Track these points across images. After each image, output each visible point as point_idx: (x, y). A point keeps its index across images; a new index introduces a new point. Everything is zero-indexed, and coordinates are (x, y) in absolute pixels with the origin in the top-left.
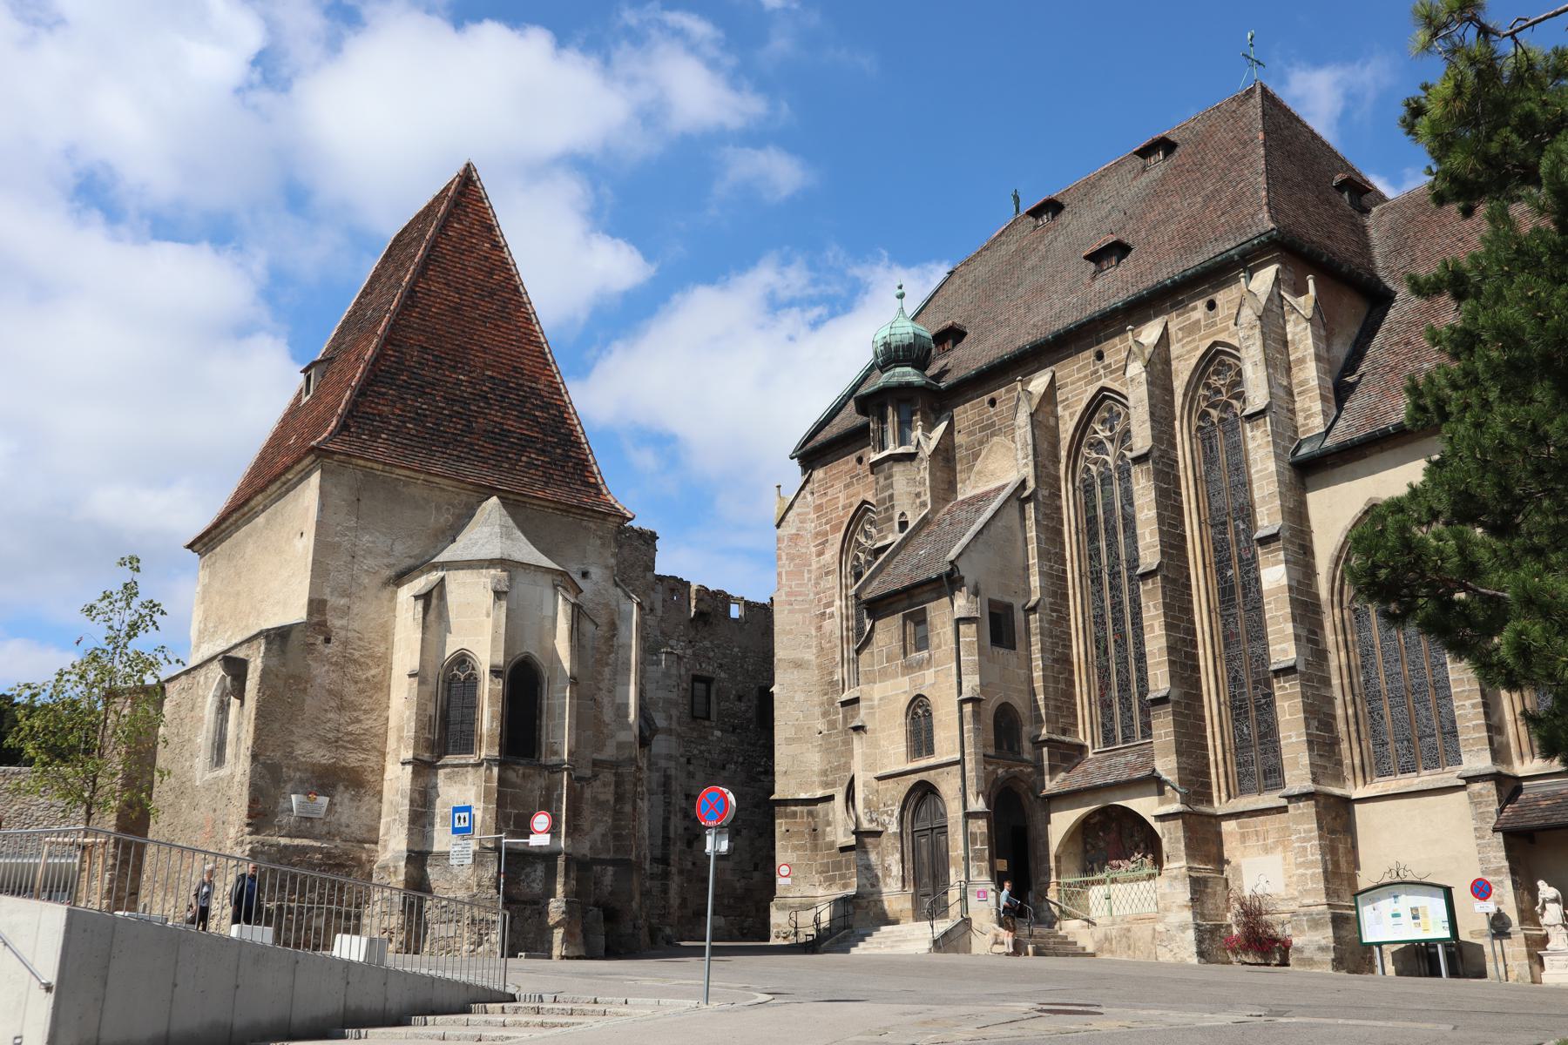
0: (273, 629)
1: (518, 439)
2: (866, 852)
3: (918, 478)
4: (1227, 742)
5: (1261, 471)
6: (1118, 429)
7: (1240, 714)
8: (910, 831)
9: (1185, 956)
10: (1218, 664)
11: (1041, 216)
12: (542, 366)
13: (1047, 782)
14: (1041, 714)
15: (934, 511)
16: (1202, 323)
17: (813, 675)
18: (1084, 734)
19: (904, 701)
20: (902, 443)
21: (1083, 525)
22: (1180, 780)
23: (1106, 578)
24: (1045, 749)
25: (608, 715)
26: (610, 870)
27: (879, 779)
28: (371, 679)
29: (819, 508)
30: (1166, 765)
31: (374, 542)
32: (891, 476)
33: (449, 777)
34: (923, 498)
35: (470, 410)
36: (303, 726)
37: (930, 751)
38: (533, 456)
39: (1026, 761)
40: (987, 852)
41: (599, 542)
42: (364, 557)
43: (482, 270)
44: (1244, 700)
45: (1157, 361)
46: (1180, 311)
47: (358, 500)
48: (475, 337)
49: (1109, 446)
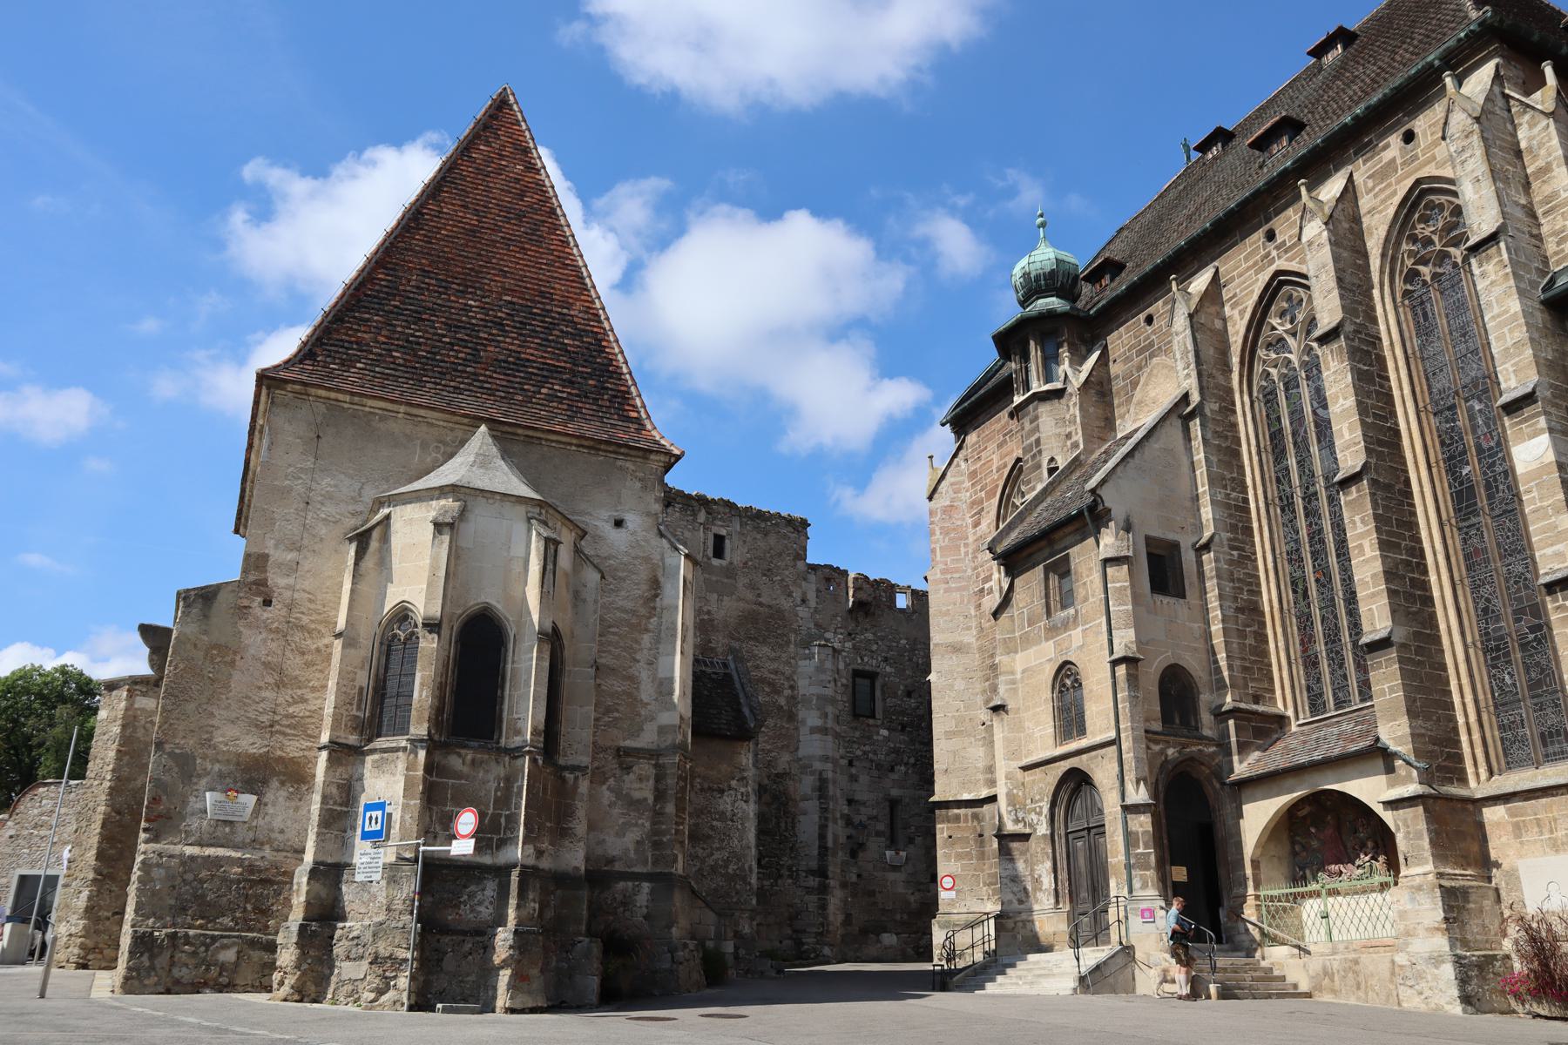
0: (194, 589)
1: (539, 369)
2: (1012, 860)
3: (1068, 417)
4: (1481, 697)
5: (1499, 316)
6: (1300, 317)
7: (1497, 658)
8: (1063, 833)
9: (1442, 1002)
10: (1460, 592)
11: (1210, 149)
12: (578, 291)
13: (1236, 764)
14: (1223, 678)
15: (1088, 451)
16: (1399, 161)
17: (974, 660)
18: (1282, 703)
19: (1049, 671)
20: (1048, 380)
21: (1266, 442)
22: (1416, 752)
23: (1299, 503)
24: (1231, 722)
25: (647, 692)
26: (646, 886)
27: (1025, 768)
28: (324, 649)
29: (973, 474)
30: (1395, 732)
31: (336, 486)
32: (1036, 418)
33: (377, 766)
34: (1074, 438)
35: (481, 338)
36: (228, 708)
37: (1082, 731)
38: (556, 387)
39: (1207, 738)
40: (1153, 858)
41: (638, 485)
42: (322, 504)
43: (511, 193)
44: (1502, 638)
45: (1342, 218)
46: (1368, 155)
47: (318, 437)
48: (494, 261)
49: (1290, 341)
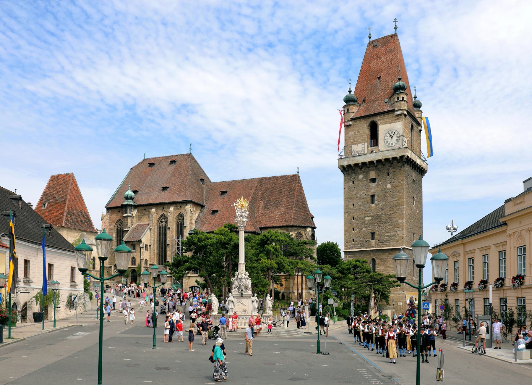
29: (110, 218)
37: (135, 265)
